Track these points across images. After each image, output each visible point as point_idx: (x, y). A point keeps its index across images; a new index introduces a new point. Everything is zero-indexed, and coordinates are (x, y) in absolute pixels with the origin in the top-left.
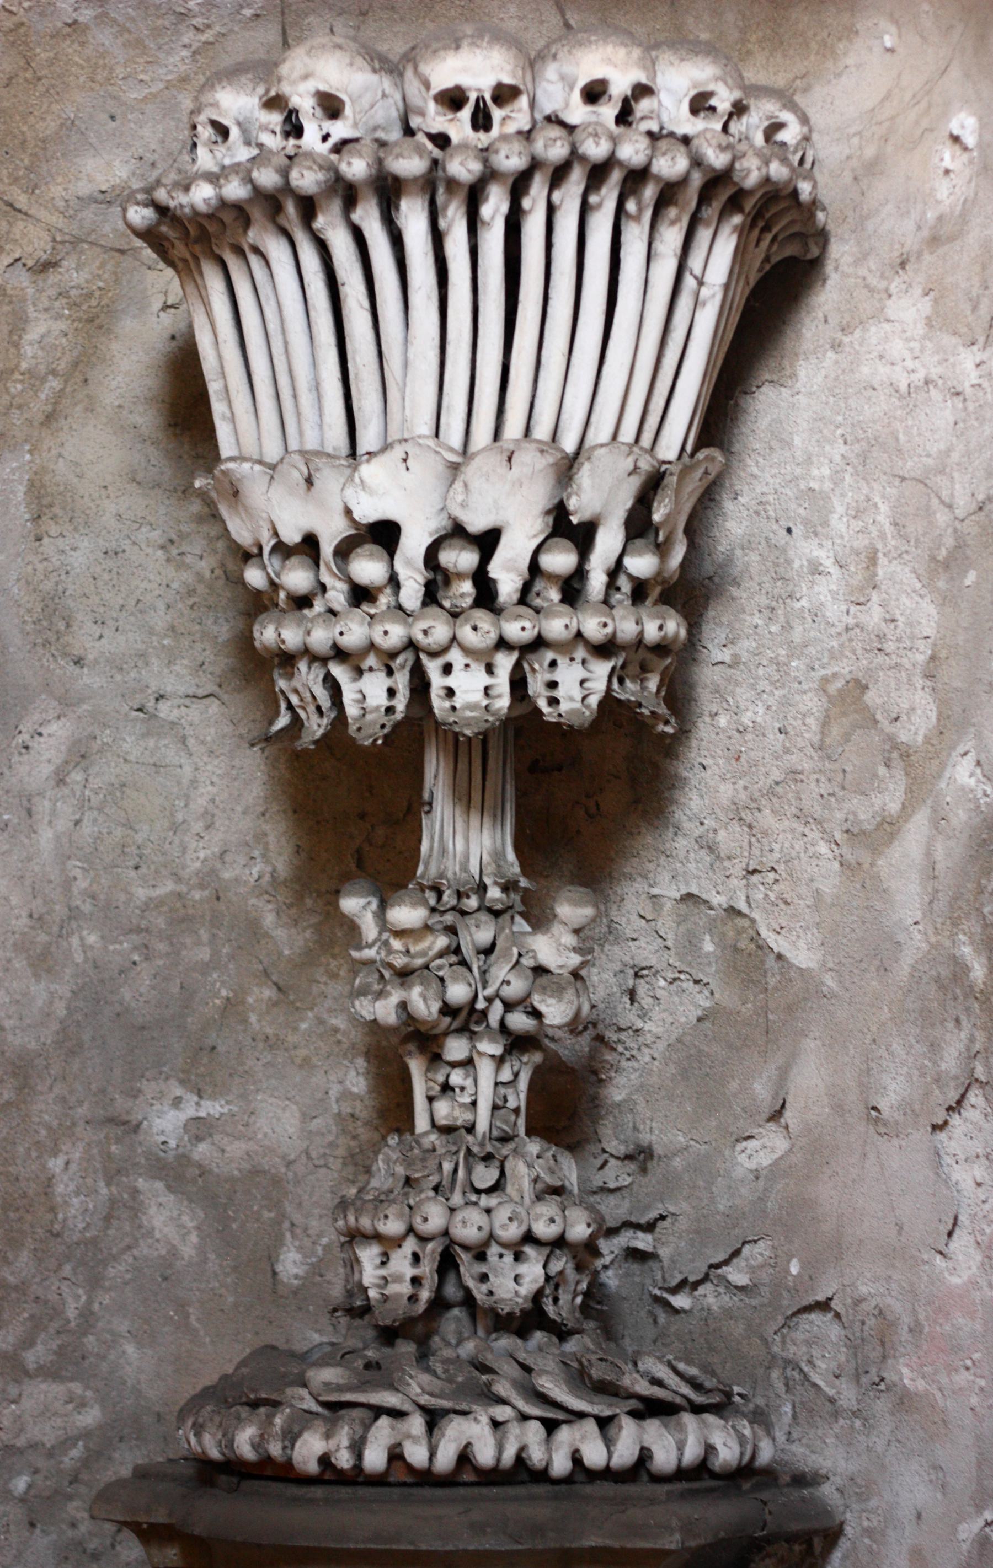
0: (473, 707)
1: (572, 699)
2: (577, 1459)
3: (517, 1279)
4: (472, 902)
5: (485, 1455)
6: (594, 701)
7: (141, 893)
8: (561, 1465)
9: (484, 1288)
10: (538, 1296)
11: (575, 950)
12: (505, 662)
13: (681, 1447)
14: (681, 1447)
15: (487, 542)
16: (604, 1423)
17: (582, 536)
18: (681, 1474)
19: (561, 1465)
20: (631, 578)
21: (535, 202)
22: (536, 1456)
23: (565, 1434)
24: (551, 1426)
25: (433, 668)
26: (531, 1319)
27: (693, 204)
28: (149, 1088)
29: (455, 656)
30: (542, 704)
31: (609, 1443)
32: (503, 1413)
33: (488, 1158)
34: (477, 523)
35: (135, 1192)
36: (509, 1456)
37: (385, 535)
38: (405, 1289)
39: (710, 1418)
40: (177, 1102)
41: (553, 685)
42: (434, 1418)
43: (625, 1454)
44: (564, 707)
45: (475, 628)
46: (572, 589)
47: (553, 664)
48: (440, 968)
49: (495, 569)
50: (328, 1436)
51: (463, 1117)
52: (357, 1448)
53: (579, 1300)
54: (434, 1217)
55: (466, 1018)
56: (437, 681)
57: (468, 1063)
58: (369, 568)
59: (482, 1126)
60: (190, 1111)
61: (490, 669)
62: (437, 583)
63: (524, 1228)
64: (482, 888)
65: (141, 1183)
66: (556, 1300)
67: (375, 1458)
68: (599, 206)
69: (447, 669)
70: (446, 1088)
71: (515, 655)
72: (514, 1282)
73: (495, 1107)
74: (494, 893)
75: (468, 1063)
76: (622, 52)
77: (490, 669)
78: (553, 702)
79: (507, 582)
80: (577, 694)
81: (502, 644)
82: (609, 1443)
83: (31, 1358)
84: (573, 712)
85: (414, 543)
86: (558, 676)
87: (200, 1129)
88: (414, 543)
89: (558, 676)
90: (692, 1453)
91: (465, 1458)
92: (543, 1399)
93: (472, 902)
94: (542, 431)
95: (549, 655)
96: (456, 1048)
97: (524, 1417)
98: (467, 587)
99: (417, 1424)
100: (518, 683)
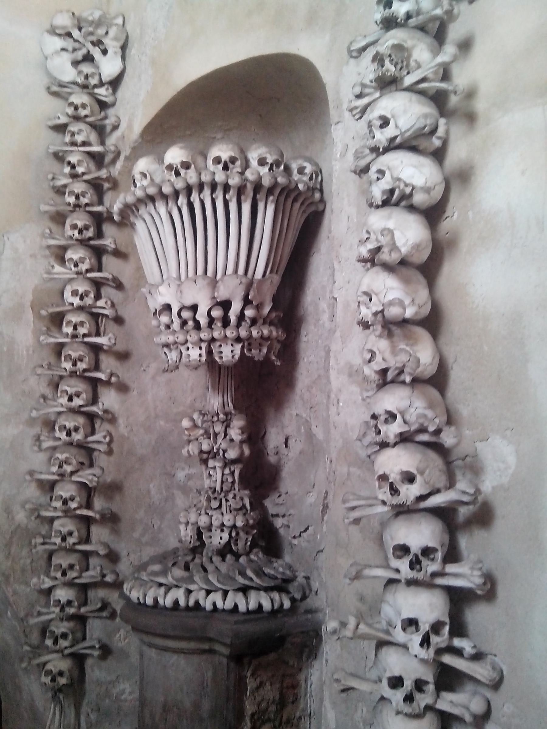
0: (195, 360)
1: (227, 356)
2: (214, 604)
3: (221, 538)
4: (215, 419)
5: (182, 603)
6: (237, 357)
7: (175, 410)
8: (209, 606)
9: (209, 540)
10: (229, 543)
11: (239, 435)
12: (204, 345)
13: (247, 603)
14: (247, 603)
15: (194, 308)
16: (225, 593)
17: (226, 305)
18: (248, 612)
19: (209, 606)
20: (249, 318)
21: (195, 198)
22: (201, 602)
23: (212, 596)
24: (208, 592)
25: (183, 348)
26: (224, 551)
27: (251, 194)
28: (177, 465)
29: (189, 345)
30: (217, 359)
31: (224, 600)
32: (192, 587)
33: (215, 498)
34: (188, 302)
35: (173, 494)
36: (191, 603)
37: (168, 308)
38: (189, 539)
39: (262, 593)
40: (183, 469)
41: (221, 352)
42: (168, 588)
43: (229, 605)
44: (224, 359)
45: (190, 336)
46: (226, 322)
47: (221, 346)
48: (201, 439)
49: (198, 317)
50: (139, 591)
51: (213, 485)
52: (145, 596)
53: (249, 543)
54: (193, 518)
55: (212, 454)
56: (184, 352)
57: (215, 468)
58: (164, 319)
59: (218, 489)
60: (187, 471)
61: (201, 348)
62: (184, 323)
63: (221, 522)
64: (218, 414)
65: (175, 492)
66: (236, 545)
67: (149, 601)
68: (217, 197)
69: (188, 349)
70: (210, 475)
71: (207, 343)
72: (218, 539)
73: (222, 482)
74: (221, 416)
75: (215, 468)
76: (225, 146)
77: (201, 348)
78: (221, 358)
79: (203, 321)
80: (230, 355)
81: (201, 340)
82: (224, 600)
83: (144, 540)
84: (227, 361)
85: (175, 310)
86: (222, 349)
87: (189, 477)
88: (175, 310)
89: (222, 349)
90: (252, 605)
91: (176, 603)
92: (208, 582)
93: (215, 419)
94: (210, 273)
95: (218, 344)
96: (211, 463)
97: (202, 589)
98: (191, 323)
99: (162, 590)
100: (210, 352)
